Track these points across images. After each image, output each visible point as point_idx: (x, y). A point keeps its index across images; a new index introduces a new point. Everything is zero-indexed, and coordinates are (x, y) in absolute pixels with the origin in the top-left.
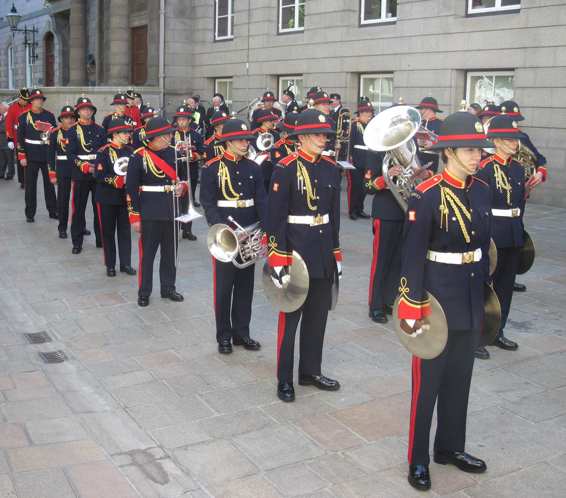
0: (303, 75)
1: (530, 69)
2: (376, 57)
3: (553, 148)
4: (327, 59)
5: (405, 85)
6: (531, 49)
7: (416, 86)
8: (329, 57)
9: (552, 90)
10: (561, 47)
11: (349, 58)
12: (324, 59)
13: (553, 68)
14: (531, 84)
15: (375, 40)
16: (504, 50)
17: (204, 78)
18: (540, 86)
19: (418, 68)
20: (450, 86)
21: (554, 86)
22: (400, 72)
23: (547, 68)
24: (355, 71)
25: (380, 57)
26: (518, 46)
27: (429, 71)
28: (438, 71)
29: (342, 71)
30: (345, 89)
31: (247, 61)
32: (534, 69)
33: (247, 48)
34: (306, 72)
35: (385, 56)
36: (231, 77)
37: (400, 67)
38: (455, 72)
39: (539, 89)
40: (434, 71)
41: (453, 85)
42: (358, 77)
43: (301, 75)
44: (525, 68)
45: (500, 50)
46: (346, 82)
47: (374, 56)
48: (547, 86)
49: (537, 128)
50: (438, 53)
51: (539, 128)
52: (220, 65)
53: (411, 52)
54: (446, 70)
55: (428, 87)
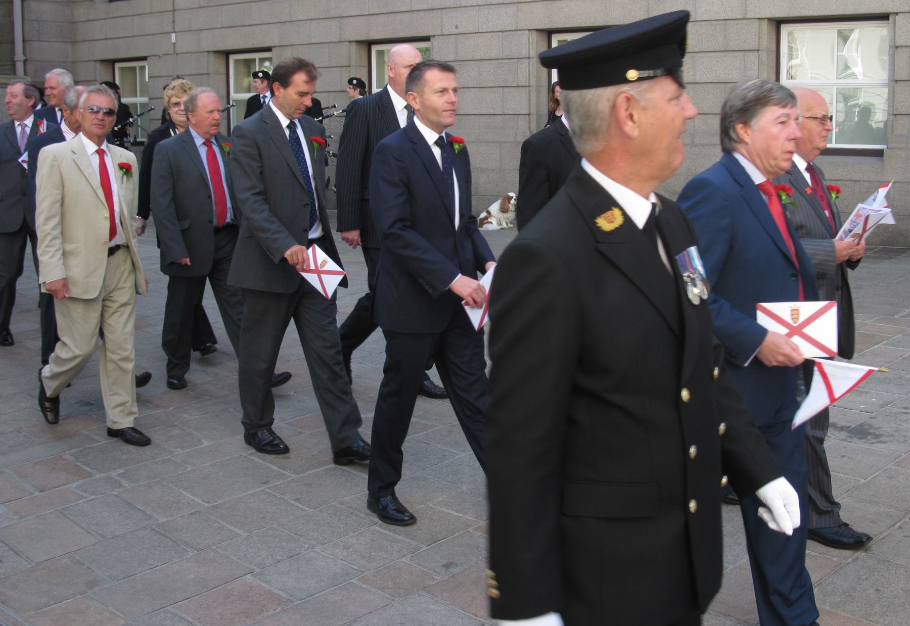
0: (273, 49)
2: (399, 16)
3: (702, 145)
4: (315, 21)
8: (317, 17)
9: (694, 57)
12: (308, 22)
17: (95, 61)
19: (471, 29)
22: (441, 37)
24: (363, 38)
25: (406, 15)
27: (492, 33)
29: (342, 40)
30: (348, 68)
31: (172, 31)
33: (172, 9)
34: (277, 44)
35: (415, 12)
36: (144, 59)
37: (442, 30)
38: (535, 33)
40: (501, 34)
42: (366, 49)
43: (269, 49)
46: (349, 58)
47: (396, 14)
50: (505, 5)
52: (123, 39)
53: (458, 6)
54: (520, 32)
55: (491, 59)
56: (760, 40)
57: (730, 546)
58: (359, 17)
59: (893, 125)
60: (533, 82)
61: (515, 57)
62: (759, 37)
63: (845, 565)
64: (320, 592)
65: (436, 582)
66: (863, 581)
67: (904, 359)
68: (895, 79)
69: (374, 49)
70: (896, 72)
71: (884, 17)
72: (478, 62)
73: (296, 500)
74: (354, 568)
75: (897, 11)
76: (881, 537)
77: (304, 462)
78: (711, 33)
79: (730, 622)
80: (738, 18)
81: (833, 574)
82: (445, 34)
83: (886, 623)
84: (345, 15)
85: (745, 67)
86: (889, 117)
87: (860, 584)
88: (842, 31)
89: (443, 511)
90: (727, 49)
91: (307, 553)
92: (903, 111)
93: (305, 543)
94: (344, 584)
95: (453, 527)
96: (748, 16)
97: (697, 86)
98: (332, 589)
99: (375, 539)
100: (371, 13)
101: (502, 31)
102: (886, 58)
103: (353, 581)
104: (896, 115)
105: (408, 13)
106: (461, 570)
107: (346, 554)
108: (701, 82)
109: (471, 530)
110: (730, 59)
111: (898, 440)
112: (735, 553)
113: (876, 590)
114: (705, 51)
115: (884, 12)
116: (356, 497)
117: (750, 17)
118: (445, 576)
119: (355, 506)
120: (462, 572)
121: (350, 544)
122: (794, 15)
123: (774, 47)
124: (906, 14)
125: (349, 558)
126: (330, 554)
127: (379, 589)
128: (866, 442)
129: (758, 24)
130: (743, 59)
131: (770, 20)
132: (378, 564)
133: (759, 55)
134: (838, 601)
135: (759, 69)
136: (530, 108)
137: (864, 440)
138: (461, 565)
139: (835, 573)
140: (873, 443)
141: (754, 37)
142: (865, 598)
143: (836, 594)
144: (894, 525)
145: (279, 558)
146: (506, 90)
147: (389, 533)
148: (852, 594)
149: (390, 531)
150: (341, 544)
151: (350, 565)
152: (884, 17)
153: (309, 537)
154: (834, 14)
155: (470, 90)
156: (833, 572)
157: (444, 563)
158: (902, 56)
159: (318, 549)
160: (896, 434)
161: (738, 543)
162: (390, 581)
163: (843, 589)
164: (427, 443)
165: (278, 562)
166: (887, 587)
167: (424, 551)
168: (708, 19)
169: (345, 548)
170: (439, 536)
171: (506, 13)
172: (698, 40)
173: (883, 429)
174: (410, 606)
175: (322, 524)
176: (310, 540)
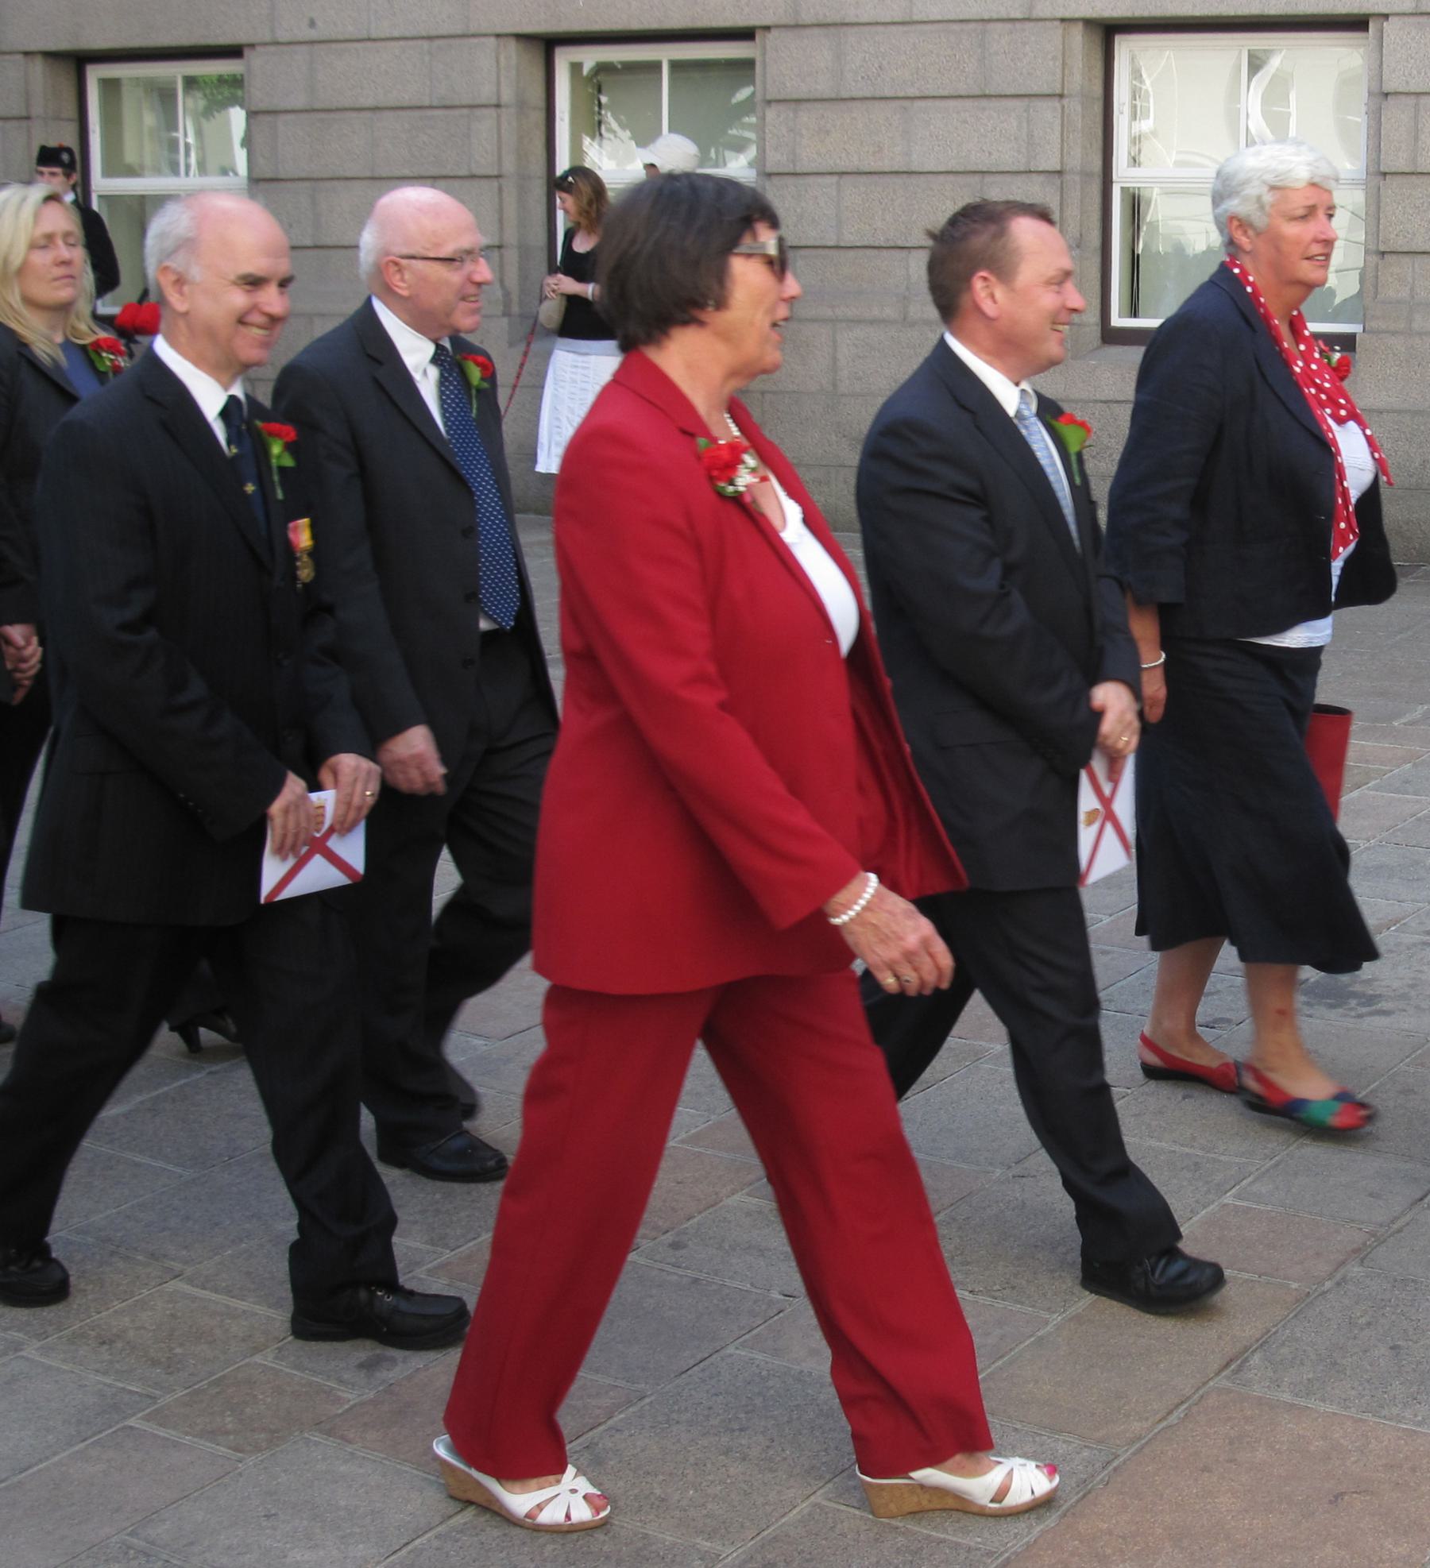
1: (816, 31)
5: (299, 101)
7: (347, 105)
13: (905, 28)
14: (823, 86)
18: (860, 94)
19: (351, 31)
20: (494, 101)
21: (912, 92)
22: (272, 49)
23: (880, 29)
24: (64, 45)
27: (402, 43)
30: (24, 124)
32: (832, 30)
38: (512, 45)
39: (858, 104)
40: (425, 44)
41: (507, 95)
44: (797, 26)
48: (888, 93)
49: (861, 252)
51: (868, 252)
54: (475, 41)
56: (1066, 72)
59: (1377, 277)
60: (509, 166)
61: (465, 102)
62: (1064, 64)
63: (1318, 1296)
64: (47, 1458)
65: (347, 1407)
66: (1362, 1329)
67: (1419, 819)
68: (1382, 169)
69: (95, 74)
70: (1383, 152)
71: (1356, 23)
72: (368, 114)
74: (131, 1392)
75: (1385, 11)
76: (1395, 1227)
79: (1064, 1446)
80: (1012, 16)
81: (1292, 1318)
82: (281, 40)
83: (1420, 1418)
85: (1030, 135)
86: (1369, 258)
87: (1355, 1338)
88: (1260, 55)
90: (987, 92)
92: (1401, 244)
94: (110, 1431)
97: (914, 180)
98: (76, 1448)
99: (179, 1314)
101: (430, 38)
102: (1359, 120)
103: (131, 1422)
104: (1383, 253)
108: (925, 170)
110: (995, 115)
111: (1418, 1007)
113: (1391, 1348)
114: (935, 94)
115: (1356, 11)
116: (119, 1213)
117: (1041, 15)
118: (367, 1391)
120: (409, 1378)
121: (115, 1331)
122: (1146, 14)
123: (1098, 89)
124: (1406, 19)
125: (117, 1366)
127: (201, 1438)
128: (1346, 1016)
129: (1060, 31)
130: (1025, 114)
131: (1089, 23)
133: (1063, 107)
134: (1309, 1380)
135: (1062, 140)
136: (501, 229)
137: (1341, 1010)
139: (1296, 1316)
140: (1360, 1016)
141: (1051, 63)
142: (1369, 1367)
143: (1303, 1364)
144: (1421, 1199)
147: (214, 1296)
148: (1338, 1361)
149: (216, 1291)
152: (1356, 23)
154: (1240, 13)
155: (348, 183)
156: (1291, 1316)
158: (1397, 115)
160: (1413, 993)
162: (229, 1413)
163: (1316, 1350)
166: (1415, 1338)
168: (939, 18)
169: (104, 1343)
172: (918, 68)
173: (1383, 983)
174: (285, 1471)
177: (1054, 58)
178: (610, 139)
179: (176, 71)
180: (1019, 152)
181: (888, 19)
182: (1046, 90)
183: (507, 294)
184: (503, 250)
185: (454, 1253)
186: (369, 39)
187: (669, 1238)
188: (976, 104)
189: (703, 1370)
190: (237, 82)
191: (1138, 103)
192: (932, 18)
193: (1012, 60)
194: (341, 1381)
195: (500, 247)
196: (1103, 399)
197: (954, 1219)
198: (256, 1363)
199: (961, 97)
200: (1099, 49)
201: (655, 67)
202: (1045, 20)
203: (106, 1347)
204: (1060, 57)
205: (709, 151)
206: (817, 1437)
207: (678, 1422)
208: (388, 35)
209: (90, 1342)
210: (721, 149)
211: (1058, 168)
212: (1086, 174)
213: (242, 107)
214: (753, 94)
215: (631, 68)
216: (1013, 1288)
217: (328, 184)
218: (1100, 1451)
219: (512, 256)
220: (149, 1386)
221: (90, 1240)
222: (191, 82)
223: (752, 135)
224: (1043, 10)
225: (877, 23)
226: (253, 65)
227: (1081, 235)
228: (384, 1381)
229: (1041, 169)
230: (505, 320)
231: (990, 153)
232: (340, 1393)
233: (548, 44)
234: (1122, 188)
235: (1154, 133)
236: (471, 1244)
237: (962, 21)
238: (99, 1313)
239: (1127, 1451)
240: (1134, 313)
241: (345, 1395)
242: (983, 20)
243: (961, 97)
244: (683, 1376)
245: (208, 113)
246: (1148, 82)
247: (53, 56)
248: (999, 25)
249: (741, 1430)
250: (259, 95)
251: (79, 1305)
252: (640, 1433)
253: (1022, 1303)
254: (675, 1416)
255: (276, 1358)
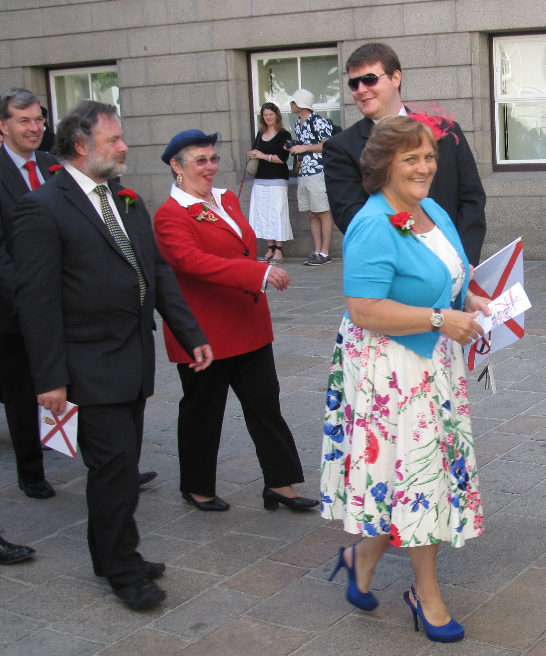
2: (79, 38)
5: (142, 82)
6: (362, 9)
10: (412, 5)
11: (25, 41)
13: (402, 39)
15: (74, 7)
16: (316, 13)
19: (162, 51)
20: (225, 79)
22: (129, 60)
25: (87, 37)
26: (340, 6)
27: (185, 55)
28: (202, 54)
29: (14, 65)
38: (232, 54)
40: (195, 55)
41: (231, 76)
44: (355, 40)
45: (309, 14)
47: (75, 36)
53: (146, 25)
57: (489, 575)
58: (31, 40)
60: (233, 106)
61: (213, 79)
62: (471, 51)
65: (187, 646)
69: (53, 75)
72: (171, 87)
73: (17, 577)
74: (93, 643)
77: (20, 534)
78: (421, 48)
79: (498, 650)
80: (448, 31)
82: (132, 56)
84: (15, 37)
85: (458, 82)
89: (183, 570)
91: (38, 633)
93: (34, 623)
95: (197, 586)
96: (459, 30)
100: (46, 35)
101: (196, 52)
105: (89, 34)
106: (211, 630)
107: (82, 628)
109: (216, 586)
112: (495, 581)
116: (85, 566)
117: (461, 30)
118: (195, 638)
119: (85, 575)
120: (212, 632)
121: (85, 617)
122: (506, 28)
123: (487, 61)
125: (87, 632)
126: (64, 631)
129: (469, 37)
130: (455, 74)
131: (481, 33)
132: (120, 634)
133: (472, 70)
136: (231, 134)
138: (211, 624)
141: (466, 51)
145: (5, 642)
146: (204, 116)
150: (76, 618)
151: (88, 640)
153: (37, 616)
155: (164, 117)
157: (192, 625)
159: (50, 627)
161: (496, 571)
162: (136, 650)
164: (157, 501)
165: (6, 647)
167: (168, 615)
168: (417, 34)
169: (81, 622)
170: (184, 598)
171: (200, 32)
175: (51, 600)
176: (38, 618)
177: (467, 49)
178: (276, 93)
179: (88, 72)
180: (454, 90)
181: (395, 35)
182: (464, 62)
183: (235, 162)
184: (232, 143)
185: (229, 577)
186: (170, 54)
187: (323, 567)
188: (434, 70)
189: (340, 624)
190: (114, 75)
191: (504, 67)
192: (413, 34)
193: (449, 50)
194: (184, 635)
195: (231, 141)
196: (495, 195)
197: (446, 554)
198: (146, 628)
199: (428, 67)
200: (486, 44)
201: (294, 60)
202: (463, 32)
203: (82, 624)
204: (469, 48)
205: (319, 96)
206: (390, 650)
207: (330, 647)
208: (179, 52)
209: (75, 622)
210: (324, 95)
211: (471, 97)
212: (483, 99)
213: (117, 86)
214: (337, 70)
215: (284, 61)
216: (473, 582)
217: (155, 118)
218: (513, 651)
219: (236, 145)
220: (101, 640)
221: (73, 578)
222: (95, 77)
223: (338, 89)
224: (461, 28)
225: (390, 37)
226: (121, 68)
227: (482, 125)
228: (202, 634)
229: (463, 97)
230: (234, 173)
231: (441, 91)
232: (183, 640)
233: (248, 53)
234: (499, 104)
235: (512, 79)
236: (237, 573)
237: (426, 35)
238: (78, 609)
239: (525, 651)
240: (507, 158)
241: (185, 641)
242: (435, 34)
243: (428, 67)
244: (332, 626)
245: (102, 89)
246: (508, 57)
247: (34, 68)
248: (443, 36)
249: (357, 649)
250: (124, 80)
251: (70, 606)
252: (314, 652)
253: (477, 589)
254: (328, 644)
255: (155, 626)
